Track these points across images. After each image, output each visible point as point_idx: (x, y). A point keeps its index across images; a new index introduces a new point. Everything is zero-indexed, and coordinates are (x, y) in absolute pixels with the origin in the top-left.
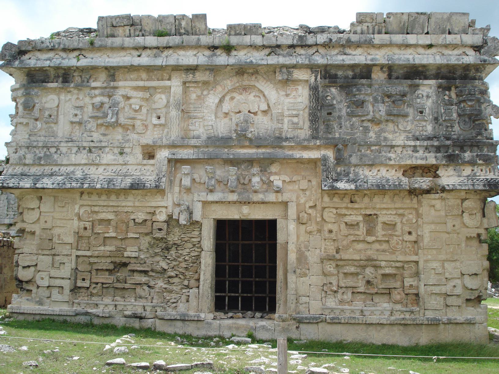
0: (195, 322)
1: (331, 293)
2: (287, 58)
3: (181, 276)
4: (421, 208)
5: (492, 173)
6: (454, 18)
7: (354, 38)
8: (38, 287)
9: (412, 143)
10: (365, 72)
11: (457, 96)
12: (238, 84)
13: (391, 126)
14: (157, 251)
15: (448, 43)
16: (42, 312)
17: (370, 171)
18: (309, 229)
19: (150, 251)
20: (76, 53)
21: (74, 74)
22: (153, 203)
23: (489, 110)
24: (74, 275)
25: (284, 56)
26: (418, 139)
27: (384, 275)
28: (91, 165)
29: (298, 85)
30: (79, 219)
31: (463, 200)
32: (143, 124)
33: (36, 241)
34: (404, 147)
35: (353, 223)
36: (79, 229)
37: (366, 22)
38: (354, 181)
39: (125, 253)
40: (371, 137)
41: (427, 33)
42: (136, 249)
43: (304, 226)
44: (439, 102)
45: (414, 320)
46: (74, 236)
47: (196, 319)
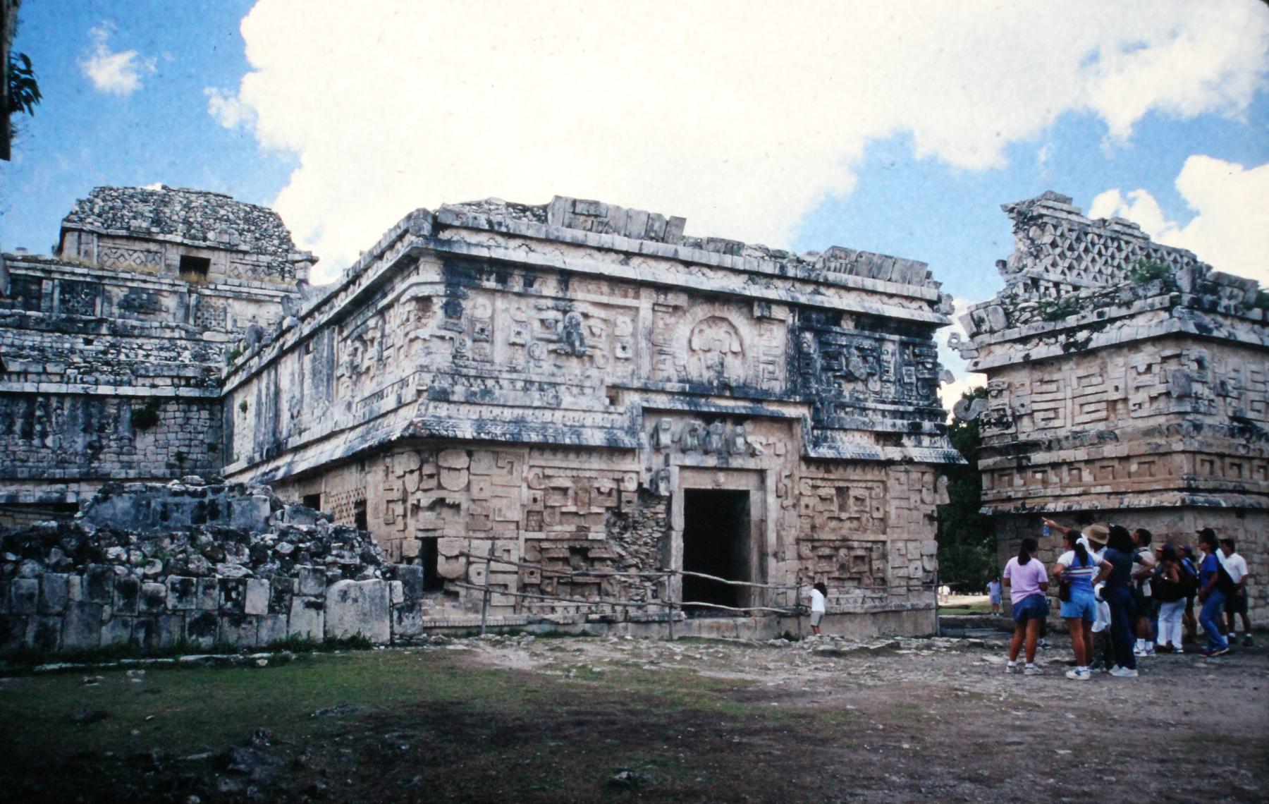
7: (832, 276)
9: (881, 406)
10: (836, 315)
18: (786, 503)
23: (941, 375)
27: (857, 558)
28: (545, 408)
30: (529, 487)
31: (923, 473)
33: (463, 519)
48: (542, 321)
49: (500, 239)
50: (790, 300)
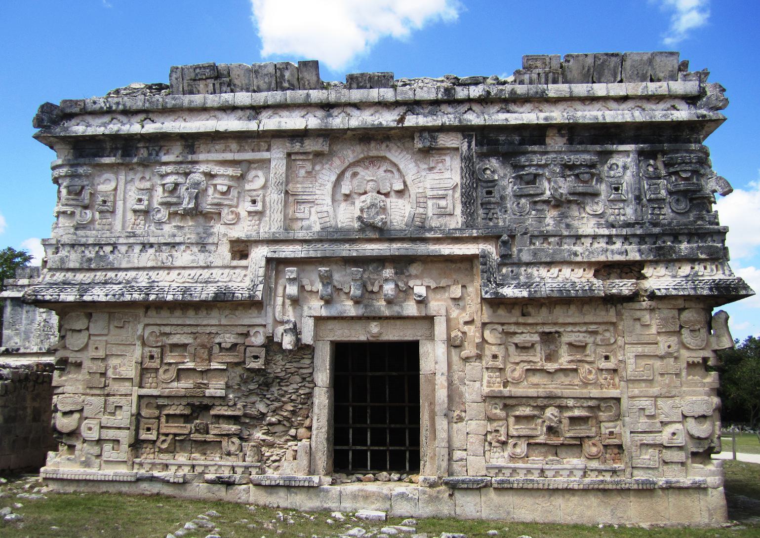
0: (305, 489)
1: (497, 444)
2: (429, 119)
3: (285, 423)
4: (622, 323)
5: (720, 272)
6: (658, 59)
8: (85, 441)
11: (667, 165)
12: (362, 156)
13: (575, 211)
14: (252, 387)
15: (650, 93)
16: (88, 478)
17: (548, 271)
18: (464, 354)
19: (243, 388)
20: (142, 117)
21: (139, 145)
22: (245, 320)
24: (134, 423)
25: (425, 116)
26: (613, 226)
27: (573, 420)
29: (445, 154)
30: (144, 344)
31: (681, 310)
32: (232, 212)
34: (595, 237)
35: (527, 345)
36: (142, 358)
37: (536, 67)
38: (527, 285)
39: (207, 391)
40: (548, 225)
41: (621, 81)
42: (222, 383)
43: (458, 350)
44: (641, 175)
45: (618, 483)
46: (136, 367)
47: (306, 484)
48: (164, 185)
49: (120, 117)
50: (457, 123)
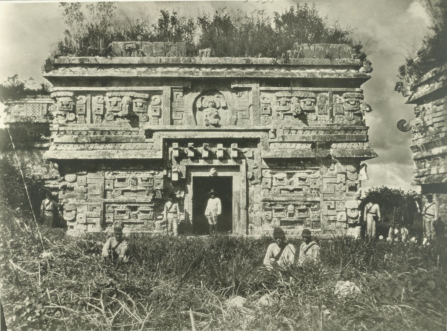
27: (300, 211)
